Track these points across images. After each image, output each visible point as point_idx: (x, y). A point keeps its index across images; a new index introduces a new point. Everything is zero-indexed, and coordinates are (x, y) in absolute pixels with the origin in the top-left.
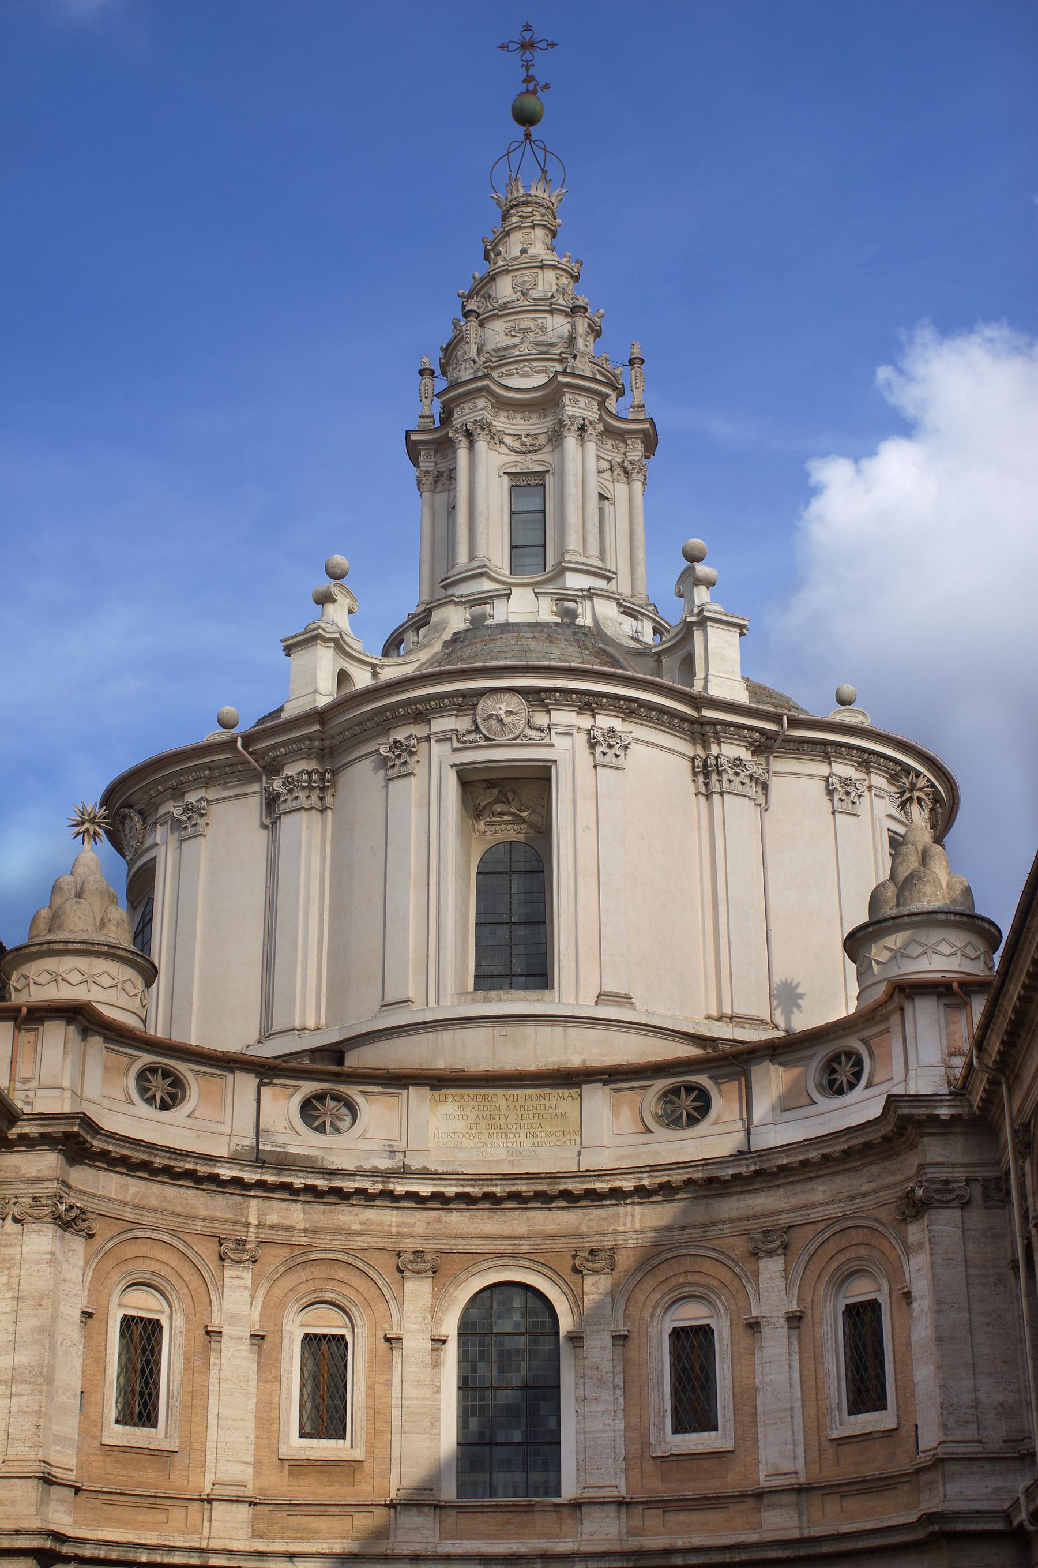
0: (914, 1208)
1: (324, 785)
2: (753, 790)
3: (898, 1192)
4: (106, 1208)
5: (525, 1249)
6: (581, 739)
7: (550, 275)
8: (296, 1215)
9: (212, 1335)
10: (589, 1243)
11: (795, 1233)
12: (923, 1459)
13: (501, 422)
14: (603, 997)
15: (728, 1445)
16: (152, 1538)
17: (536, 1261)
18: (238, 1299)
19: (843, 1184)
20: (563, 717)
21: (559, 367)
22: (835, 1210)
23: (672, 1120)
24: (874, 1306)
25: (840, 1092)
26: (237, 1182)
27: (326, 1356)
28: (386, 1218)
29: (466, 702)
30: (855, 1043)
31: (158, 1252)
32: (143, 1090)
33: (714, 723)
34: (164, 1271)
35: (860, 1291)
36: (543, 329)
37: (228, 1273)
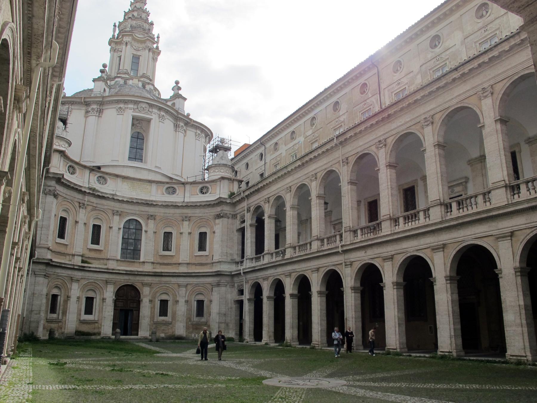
0: (219, 216)
1: (100, 112)
2: (183, 132)
3: (214, 214)
4: (61, 194)
5: (138, 213)
6: (157, 115)
7: (145, 14)
8: (93, 200)
9: (77, 222)
10: (150, 214)
11: (191, 218)
12: (214, 261)
13: (133, 42)
14: (156, 167)
15: (174, 254)
16: (63, 262)
17: (139, 215)
18: (82, 216)
19: (203, 210)
20: (155, 111)
21: (146, 35)
22: (201, 215)
23: (169, 193)
24: (206, 233)
25: (203, 193)
26: (85, 192)
27: (97, 229)
28: (112, 203)
29: (136, 103)
30: (208, 185)
31: (68, 204)
32: (68, 170)
33: (180, 118)
34: (69, 208)
35: (203, 230)
36: (143, 26)
37: (81, 210)
